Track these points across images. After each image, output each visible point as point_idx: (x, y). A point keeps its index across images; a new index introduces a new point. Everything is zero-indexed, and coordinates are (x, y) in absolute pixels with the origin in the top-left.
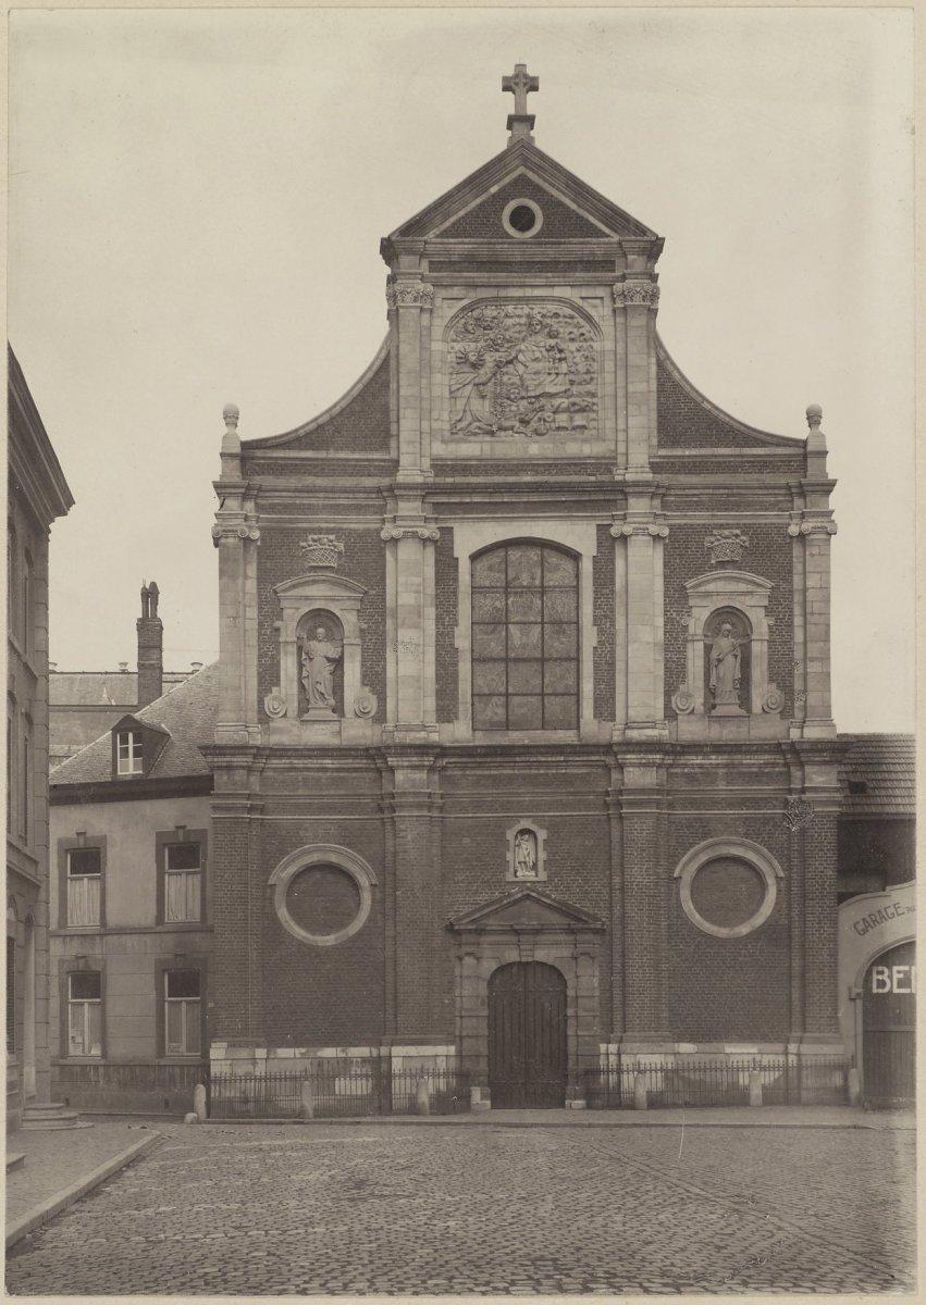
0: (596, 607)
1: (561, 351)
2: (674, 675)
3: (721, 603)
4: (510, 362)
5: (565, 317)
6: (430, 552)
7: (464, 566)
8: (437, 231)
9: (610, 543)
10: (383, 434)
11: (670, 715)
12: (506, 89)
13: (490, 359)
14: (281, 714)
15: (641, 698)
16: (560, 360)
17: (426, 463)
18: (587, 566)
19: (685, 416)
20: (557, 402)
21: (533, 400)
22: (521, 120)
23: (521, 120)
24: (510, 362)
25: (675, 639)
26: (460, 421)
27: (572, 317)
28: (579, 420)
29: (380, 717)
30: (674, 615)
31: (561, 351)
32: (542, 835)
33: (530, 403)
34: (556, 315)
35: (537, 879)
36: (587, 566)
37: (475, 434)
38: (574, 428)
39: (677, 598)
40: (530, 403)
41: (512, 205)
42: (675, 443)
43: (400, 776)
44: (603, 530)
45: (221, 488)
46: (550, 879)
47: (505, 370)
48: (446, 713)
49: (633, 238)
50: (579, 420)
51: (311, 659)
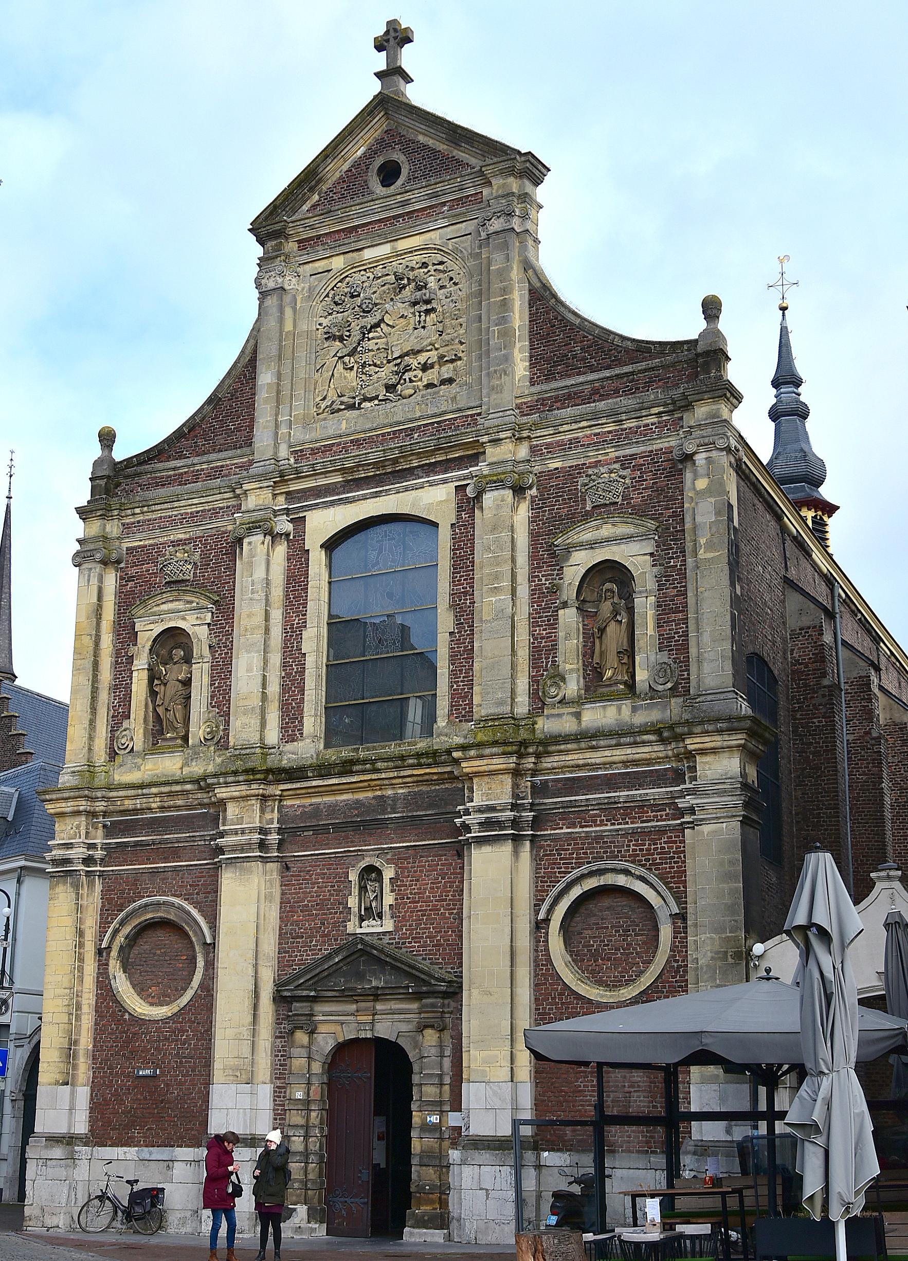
0: (454, 582)
1: (428, 302)
2: (543, 653)
3: (600, 555)
4: (377, 325)
5: (434, 264)
6: (281, 549)
7: (317, 560)
11: (539, 701)
12: (379, 47)
13: (355, 327)
14: (128, 750)
16: (427, 312)
17: (283, 452)
18: (445, 535)
19: (567, 343)
20: (422, 358)
21: (399, 360)
22: (393, 74)
23: (393, 74)
24: (377, 325)
25: (545, 602)
26: (324, 399)
27: (441, 263)
28: (447, 371)
29: (222, 744)
30: (543, 582)
31: (428, 302)
32: (389, 873)
33: (396, 365)
34: (425, 265)
35: (380, 930)
37: (340, 410)
38: (443, 382)
39: (547, 555)
40: (396, 365)
41: (379, 161)
42: (549, 377)
43: (232, 810)
44: (460, 489)
45: (83, 513)
46: (397, 929)
47: (371, 335)
48: (291, 727)
49: (495, 160)
50: (447, 371)
51: (165, 684)
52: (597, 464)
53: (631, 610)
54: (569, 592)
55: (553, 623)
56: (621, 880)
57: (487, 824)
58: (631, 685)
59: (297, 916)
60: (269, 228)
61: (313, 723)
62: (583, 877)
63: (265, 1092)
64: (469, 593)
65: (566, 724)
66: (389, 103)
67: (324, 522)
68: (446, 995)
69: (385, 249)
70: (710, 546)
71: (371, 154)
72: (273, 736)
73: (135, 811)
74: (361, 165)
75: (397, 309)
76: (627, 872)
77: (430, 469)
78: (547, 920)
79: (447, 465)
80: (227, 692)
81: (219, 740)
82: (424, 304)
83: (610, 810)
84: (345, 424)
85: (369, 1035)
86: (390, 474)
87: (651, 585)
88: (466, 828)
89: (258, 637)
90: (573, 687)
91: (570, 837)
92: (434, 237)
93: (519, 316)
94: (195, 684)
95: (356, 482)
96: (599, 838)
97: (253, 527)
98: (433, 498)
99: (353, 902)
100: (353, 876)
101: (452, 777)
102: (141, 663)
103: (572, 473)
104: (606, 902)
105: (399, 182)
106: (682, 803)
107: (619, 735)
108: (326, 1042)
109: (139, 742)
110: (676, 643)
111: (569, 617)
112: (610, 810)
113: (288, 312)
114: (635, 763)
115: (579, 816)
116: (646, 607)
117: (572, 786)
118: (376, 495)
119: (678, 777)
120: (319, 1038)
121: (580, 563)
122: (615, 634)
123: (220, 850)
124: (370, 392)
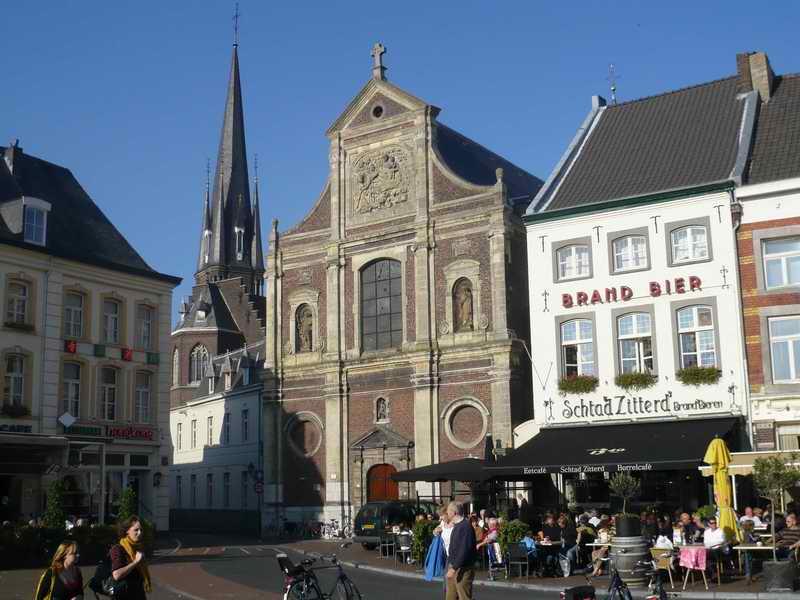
8: (347, 126)
18: (403, 265)
20: (394, 190)
25: (440, 293)
28: (403, 198)
29: (324, 351)
32: (387, 402)
36: (403, 265)
38: (403, 201)
42: (441, 201)
44: (409, 247)
52: (458, 238)
53: (472, 296)
54: (449, 290)
55: (444, 301)
56: (469, 403)
57: (421, 382)
58: (472, 326)
59: (350, 418)
61: (357, 342)
62: (455, 402)
63: (346, 484)
64: (413, 290)
65: (450, 343)
67: (359, 260)
68: (409, 447)
69: (378, 145)
70: (499, 273)
71: (371, 103)
73: (294, 377)
75: (384, 170)
76: (471, 400)
77: (398, 239)
78: (444, 418)
79: (404, 237)
80: (325, 329)
82: (395, 168)
83: (466, 376)
84: (366, 220)
85: (382, 463)
86: (383, 241)
87: (479, 287)
88: (414, 383)
89: (336, 308)
90: (451, 328)
91: (451, 387)
92: (396, 140)
94: (313, 326)
96: (462, 386)
97: (330, 263)
98: (398, 251)
99: (375, 412)
100: (375, 402)
101: (408, 363)
103: (449, 242)
104: (460, 412)
105: (384, 112)
106: (490, 373)
107: (470, 346)
108: (367, 465)
109: (293, 349)
110: (487, 310)
112: (466, 376)
113: (342, 171)
114: (474, 357)
115: (455, 378)
116: (476, 295)
117: (452, 366)
118: (378, 249)
120: (365, 463)
121: (452, 278)
123: (325, 393)
124: (374, 205)
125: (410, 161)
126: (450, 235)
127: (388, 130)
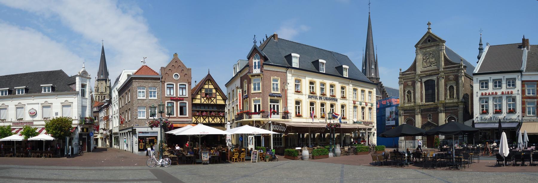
2: (446, 94)
9: (438, 79)
10: (415, 70)
11: (445, 99)
15: (442, 98)
25: (446, 89)
39: (446, 85)
60: (416, 46)
61: (424, 100)
66: (428, 32)
67: (424, 80)
72: (420, 101)
74: (426, 39)
81: (415, 102)
83: (452, 110)
84: (425, 69)
86: (430, 75)
93: (443, 59)
95: (427, 76)
98: (434, 78)
102: (406, 94)
111: (448, 91)
115: (449, 110)
116: (455, 91)
117: (448, 107)
119: (458, 107)
122: (452, 94)
125: (438, 55)
126: (448, 74)
127: (432, 46)
